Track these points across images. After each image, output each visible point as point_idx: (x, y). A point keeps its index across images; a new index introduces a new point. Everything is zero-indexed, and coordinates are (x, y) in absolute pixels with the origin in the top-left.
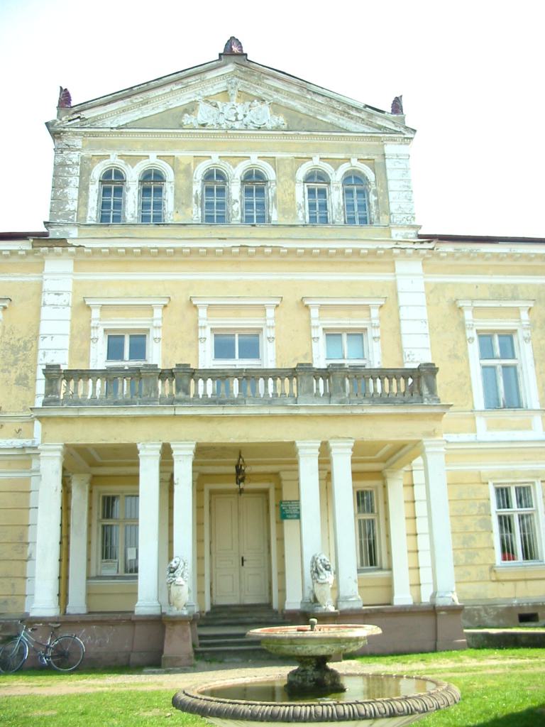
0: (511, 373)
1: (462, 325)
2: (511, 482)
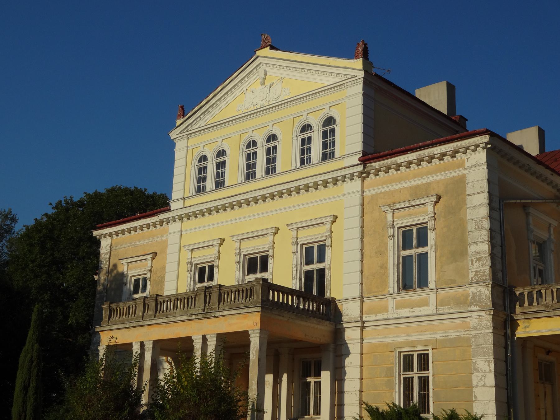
0: (423, 258)
2: (416, 350)
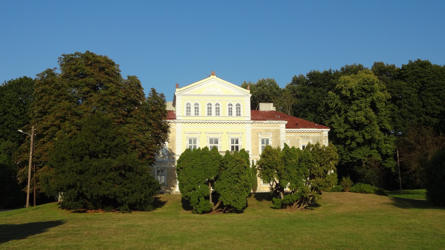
1: (258, 138)
